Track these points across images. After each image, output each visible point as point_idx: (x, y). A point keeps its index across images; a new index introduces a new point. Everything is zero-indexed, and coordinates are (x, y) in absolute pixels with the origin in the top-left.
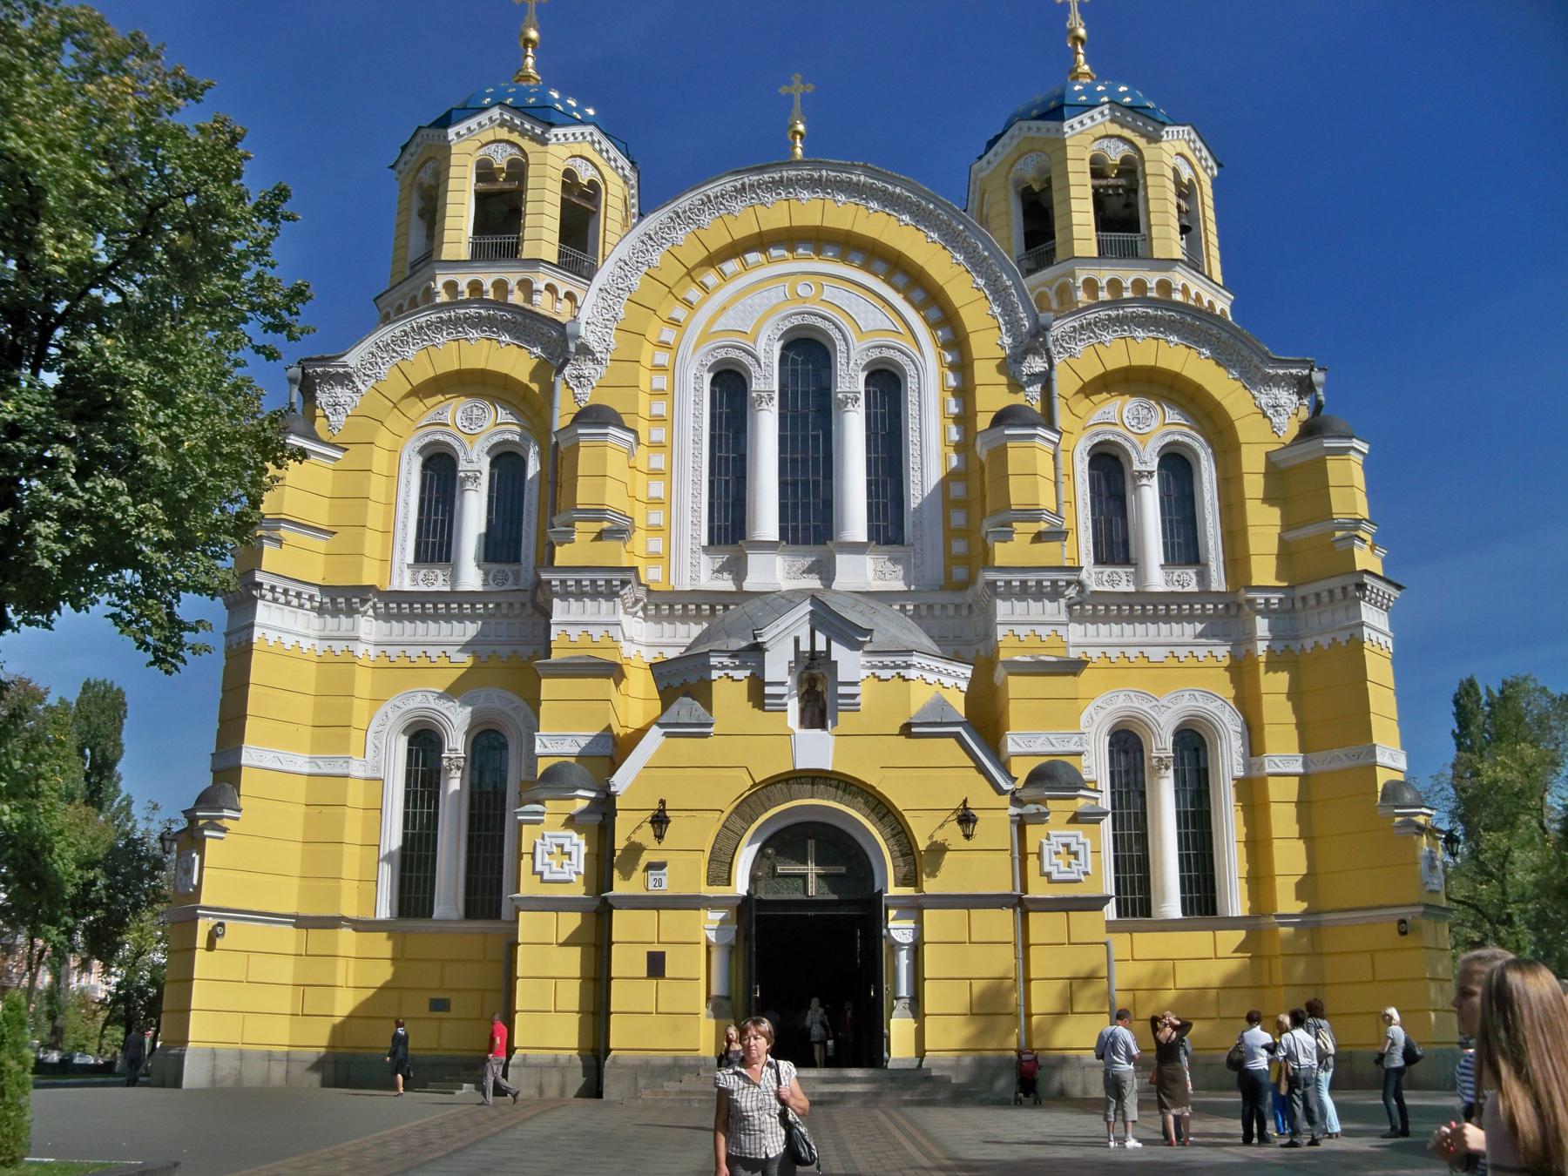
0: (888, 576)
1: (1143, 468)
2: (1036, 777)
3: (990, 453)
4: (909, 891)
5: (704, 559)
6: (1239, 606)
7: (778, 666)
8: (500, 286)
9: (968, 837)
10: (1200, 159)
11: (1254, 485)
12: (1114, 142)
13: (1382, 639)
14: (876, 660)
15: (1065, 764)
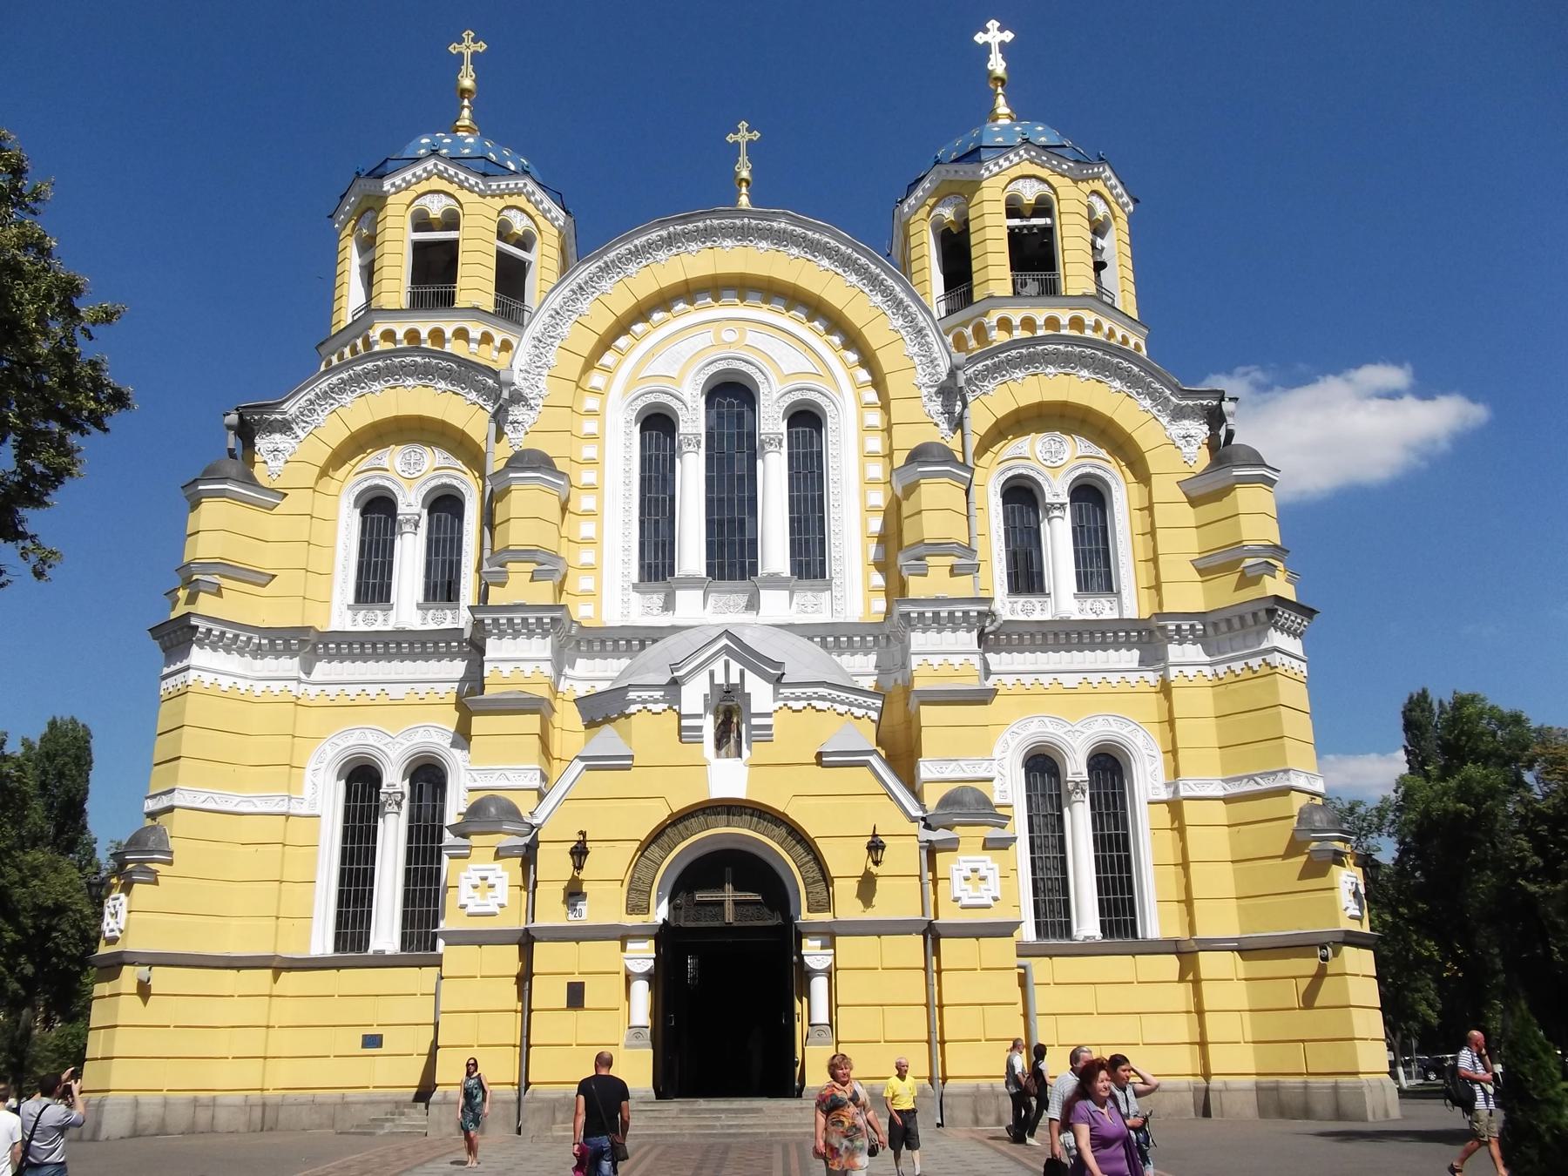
0: (810, 609)
1: (1054, 500)
2: (946, 802)
5: (635, 596)
6: (1151, 632)
8: (437, 335)
13: (1295, 663)
15: (974, 790)
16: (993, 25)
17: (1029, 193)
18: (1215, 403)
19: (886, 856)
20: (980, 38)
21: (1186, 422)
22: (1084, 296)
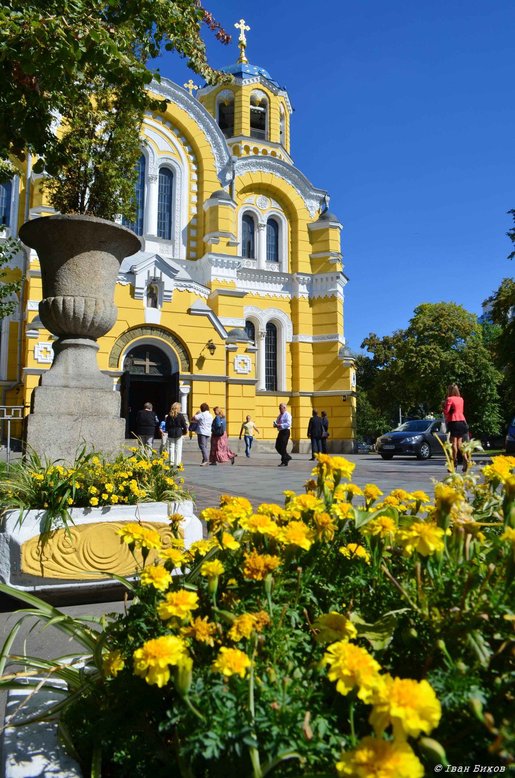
1: (262, 223)
3: (211, 208)
4: (188, 374)
7: (141, 281)
9: (212, 354)
10: (288, 106)
11: (303, 236)
12: (260, 92)
14: (178, 283)
17: (260, 96)
19: (216, 351)
20: (237, 25)
21: (312, 201)
22: (277, 143)
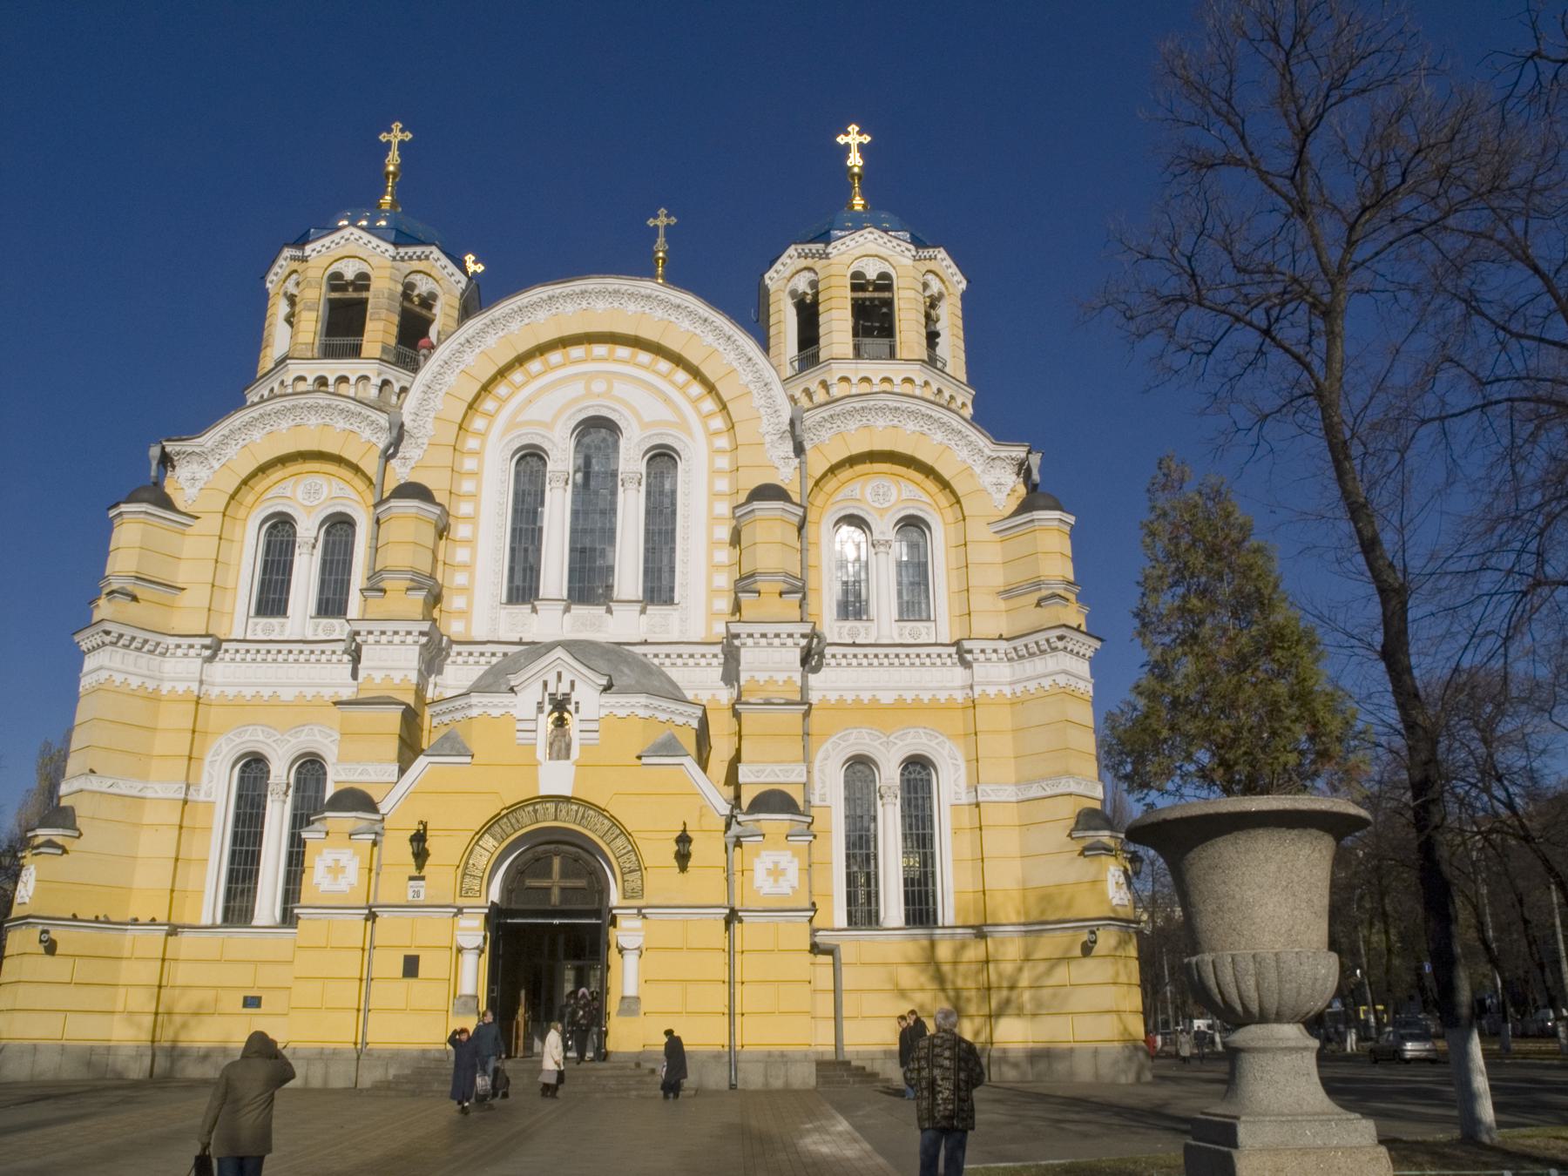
16: (853, 128)
18: (1023, 455)
